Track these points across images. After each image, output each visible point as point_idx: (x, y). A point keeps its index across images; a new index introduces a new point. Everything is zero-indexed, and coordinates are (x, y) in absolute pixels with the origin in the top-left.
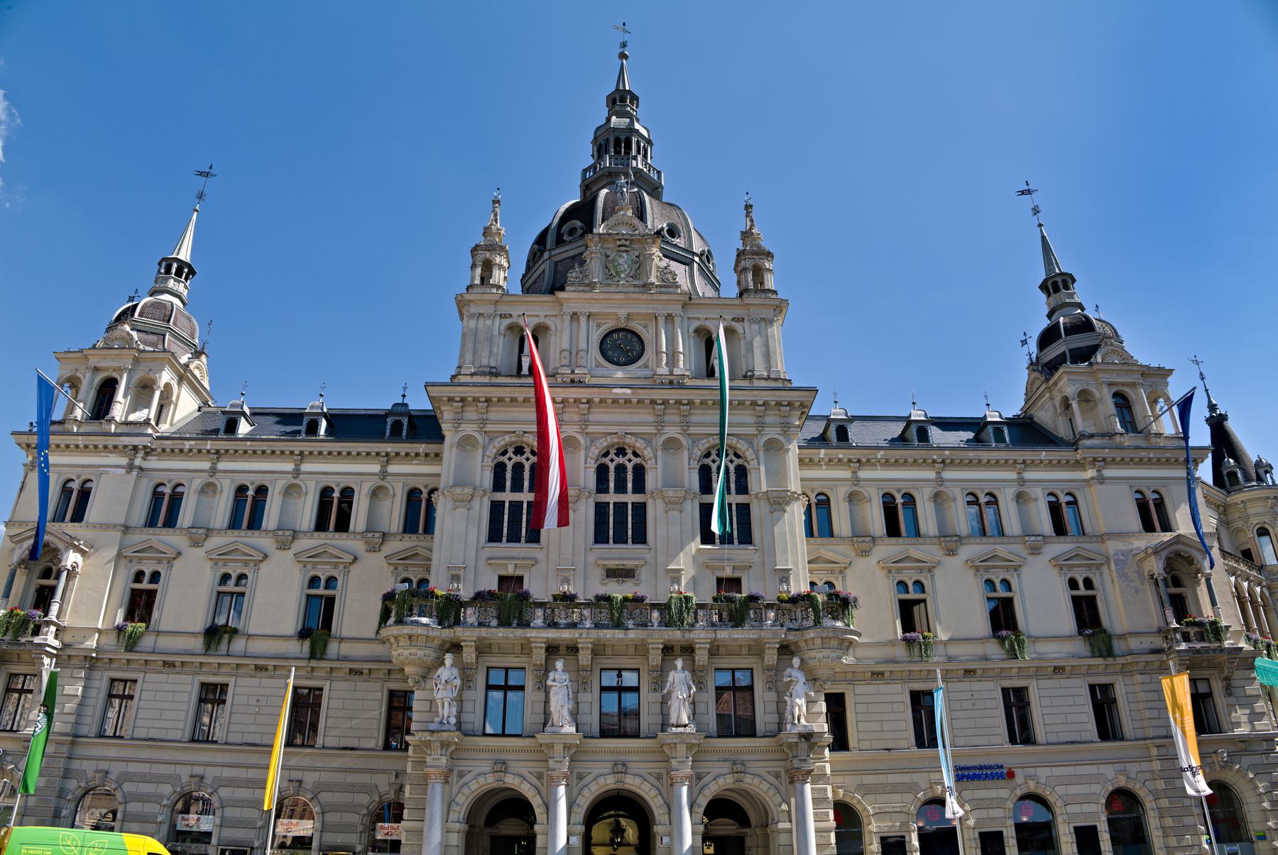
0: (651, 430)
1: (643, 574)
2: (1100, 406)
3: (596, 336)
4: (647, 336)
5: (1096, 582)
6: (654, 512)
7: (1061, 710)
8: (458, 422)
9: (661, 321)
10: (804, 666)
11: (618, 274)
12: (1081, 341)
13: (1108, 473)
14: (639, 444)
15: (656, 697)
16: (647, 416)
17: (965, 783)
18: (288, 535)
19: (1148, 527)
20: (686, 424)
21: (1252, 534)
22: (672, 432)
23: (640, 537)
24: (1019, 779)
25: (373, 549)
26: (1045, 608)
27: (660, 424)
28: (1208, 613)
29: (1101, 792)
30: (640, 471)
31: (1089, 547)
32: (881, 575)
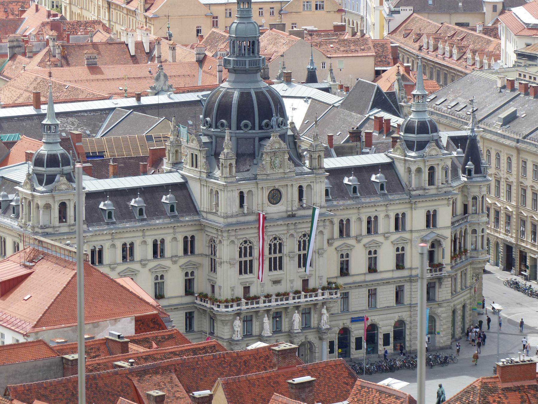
0: (286, 232)
1: (283, 282)
2: (423, 175)
3: (266, 193)
4: (283, 191)
5: (405, 249)
6: (285, 260)
7: (385, 296)
8: (229, 237)
9: (289, 186)
10: (327, 309)
11: (275, 167)
12: (423, 137)
13: (419, 205)
14: (282, 237)
15: (287, 320)
16: (285, 228)
17: (353, 323)
18: (143, 263)
19: (428, 226)
20: (295, 229)
21: (470, 200)
22: (292, 232)
23: (281, 268)
24: (369, 320)
25: (175, 262)
26: (386, 261)
27: (288, 230)
28: (441, 260)
29: (393, 323)
30: (280, 244)
31: (406, 235)
32: (335, 252)
